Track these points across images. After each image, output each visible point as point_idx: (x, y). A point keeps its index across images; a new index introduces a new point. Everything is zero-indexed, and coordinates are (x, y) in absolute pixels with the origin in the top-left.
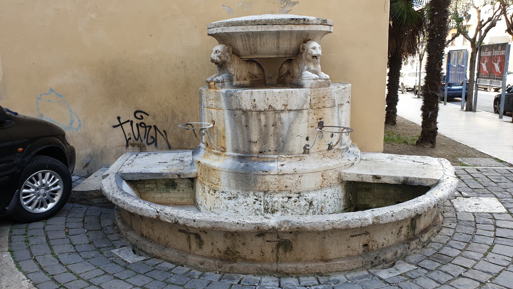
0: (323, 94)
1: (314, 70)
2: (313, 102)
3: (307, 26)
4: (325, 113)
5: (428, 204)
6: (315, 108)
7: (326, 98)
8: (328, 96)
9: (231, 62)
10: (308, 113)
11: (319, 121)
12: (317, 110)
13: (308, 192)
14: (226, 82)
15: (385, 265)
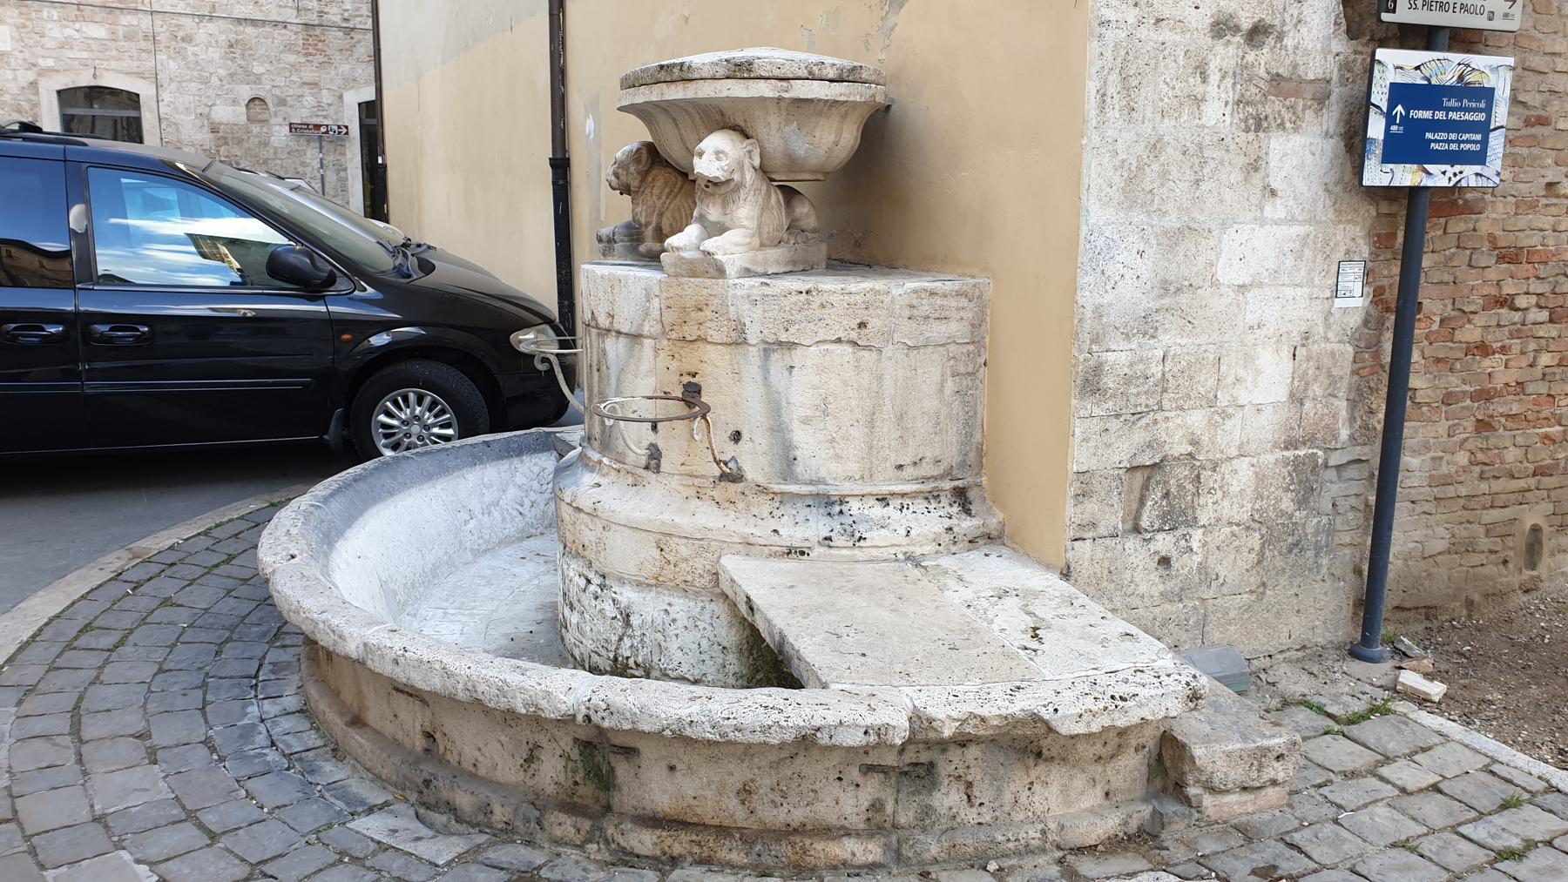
0: (694, 298)
1: (719, 223)
2: (668, 318)
3: (689, 84)
4: (705, 358)
5: (532, 693)
6: (673, 337)
7: (708, 312)
8: (713, 308)
9: (641, 190)
10: (656, 350)
11: (686, 379)
12: (682, 344)
13: (622, 581)
14: (622, 241)
15: (453, 822)
